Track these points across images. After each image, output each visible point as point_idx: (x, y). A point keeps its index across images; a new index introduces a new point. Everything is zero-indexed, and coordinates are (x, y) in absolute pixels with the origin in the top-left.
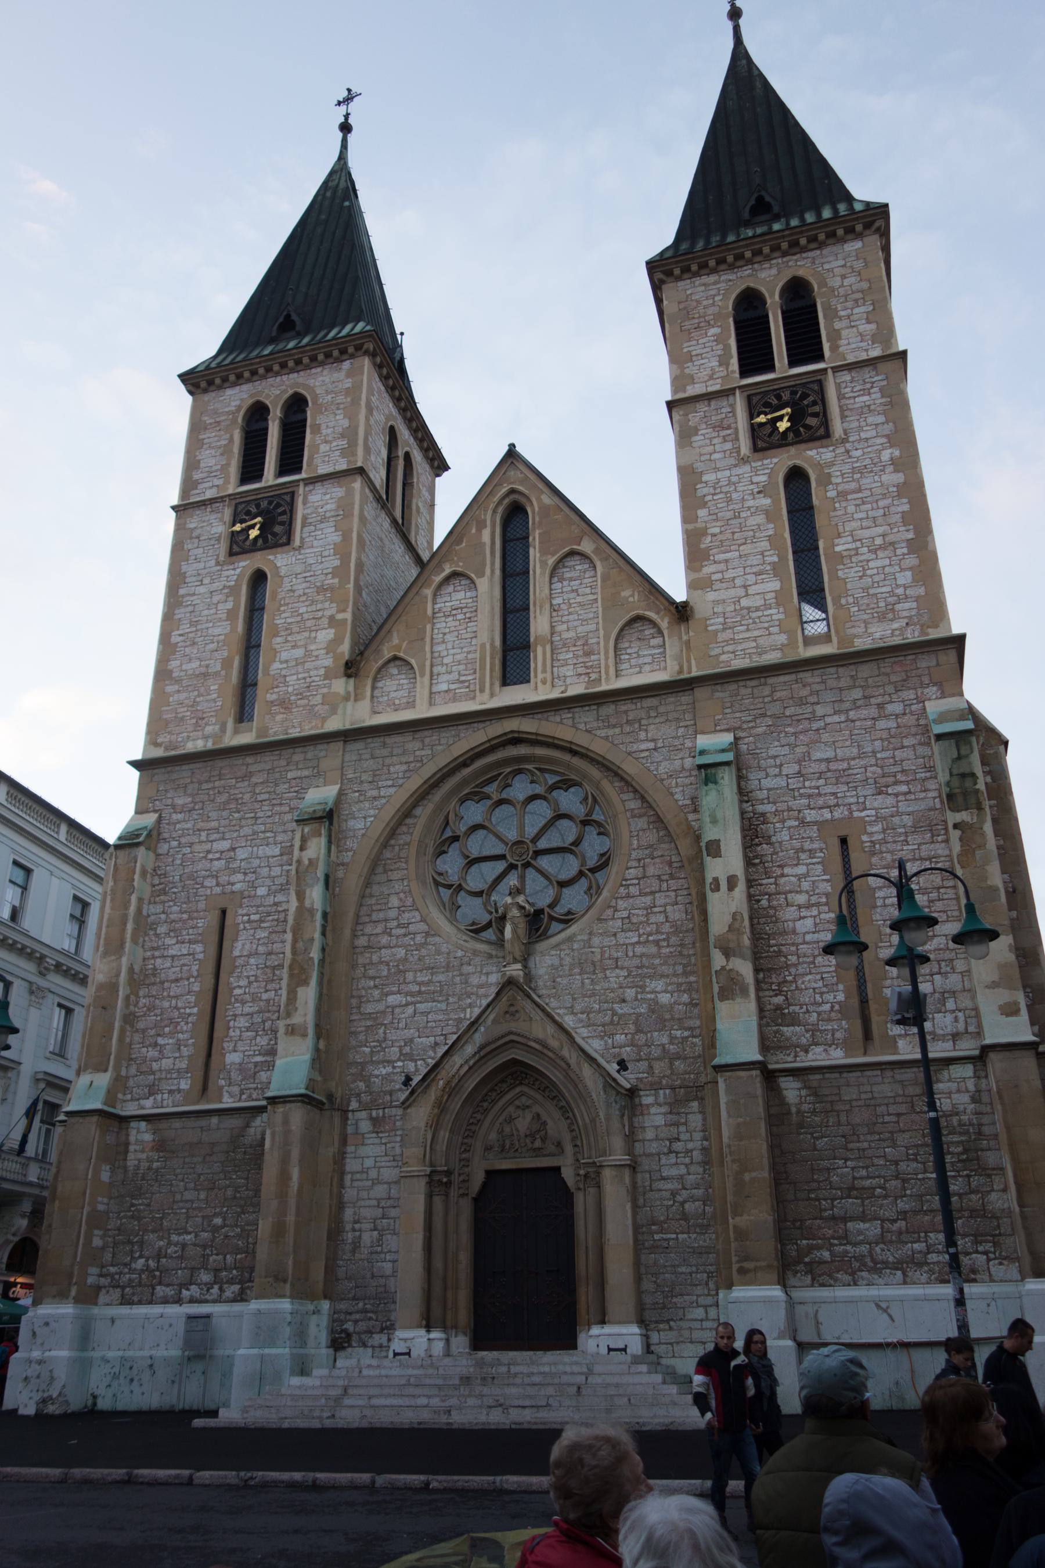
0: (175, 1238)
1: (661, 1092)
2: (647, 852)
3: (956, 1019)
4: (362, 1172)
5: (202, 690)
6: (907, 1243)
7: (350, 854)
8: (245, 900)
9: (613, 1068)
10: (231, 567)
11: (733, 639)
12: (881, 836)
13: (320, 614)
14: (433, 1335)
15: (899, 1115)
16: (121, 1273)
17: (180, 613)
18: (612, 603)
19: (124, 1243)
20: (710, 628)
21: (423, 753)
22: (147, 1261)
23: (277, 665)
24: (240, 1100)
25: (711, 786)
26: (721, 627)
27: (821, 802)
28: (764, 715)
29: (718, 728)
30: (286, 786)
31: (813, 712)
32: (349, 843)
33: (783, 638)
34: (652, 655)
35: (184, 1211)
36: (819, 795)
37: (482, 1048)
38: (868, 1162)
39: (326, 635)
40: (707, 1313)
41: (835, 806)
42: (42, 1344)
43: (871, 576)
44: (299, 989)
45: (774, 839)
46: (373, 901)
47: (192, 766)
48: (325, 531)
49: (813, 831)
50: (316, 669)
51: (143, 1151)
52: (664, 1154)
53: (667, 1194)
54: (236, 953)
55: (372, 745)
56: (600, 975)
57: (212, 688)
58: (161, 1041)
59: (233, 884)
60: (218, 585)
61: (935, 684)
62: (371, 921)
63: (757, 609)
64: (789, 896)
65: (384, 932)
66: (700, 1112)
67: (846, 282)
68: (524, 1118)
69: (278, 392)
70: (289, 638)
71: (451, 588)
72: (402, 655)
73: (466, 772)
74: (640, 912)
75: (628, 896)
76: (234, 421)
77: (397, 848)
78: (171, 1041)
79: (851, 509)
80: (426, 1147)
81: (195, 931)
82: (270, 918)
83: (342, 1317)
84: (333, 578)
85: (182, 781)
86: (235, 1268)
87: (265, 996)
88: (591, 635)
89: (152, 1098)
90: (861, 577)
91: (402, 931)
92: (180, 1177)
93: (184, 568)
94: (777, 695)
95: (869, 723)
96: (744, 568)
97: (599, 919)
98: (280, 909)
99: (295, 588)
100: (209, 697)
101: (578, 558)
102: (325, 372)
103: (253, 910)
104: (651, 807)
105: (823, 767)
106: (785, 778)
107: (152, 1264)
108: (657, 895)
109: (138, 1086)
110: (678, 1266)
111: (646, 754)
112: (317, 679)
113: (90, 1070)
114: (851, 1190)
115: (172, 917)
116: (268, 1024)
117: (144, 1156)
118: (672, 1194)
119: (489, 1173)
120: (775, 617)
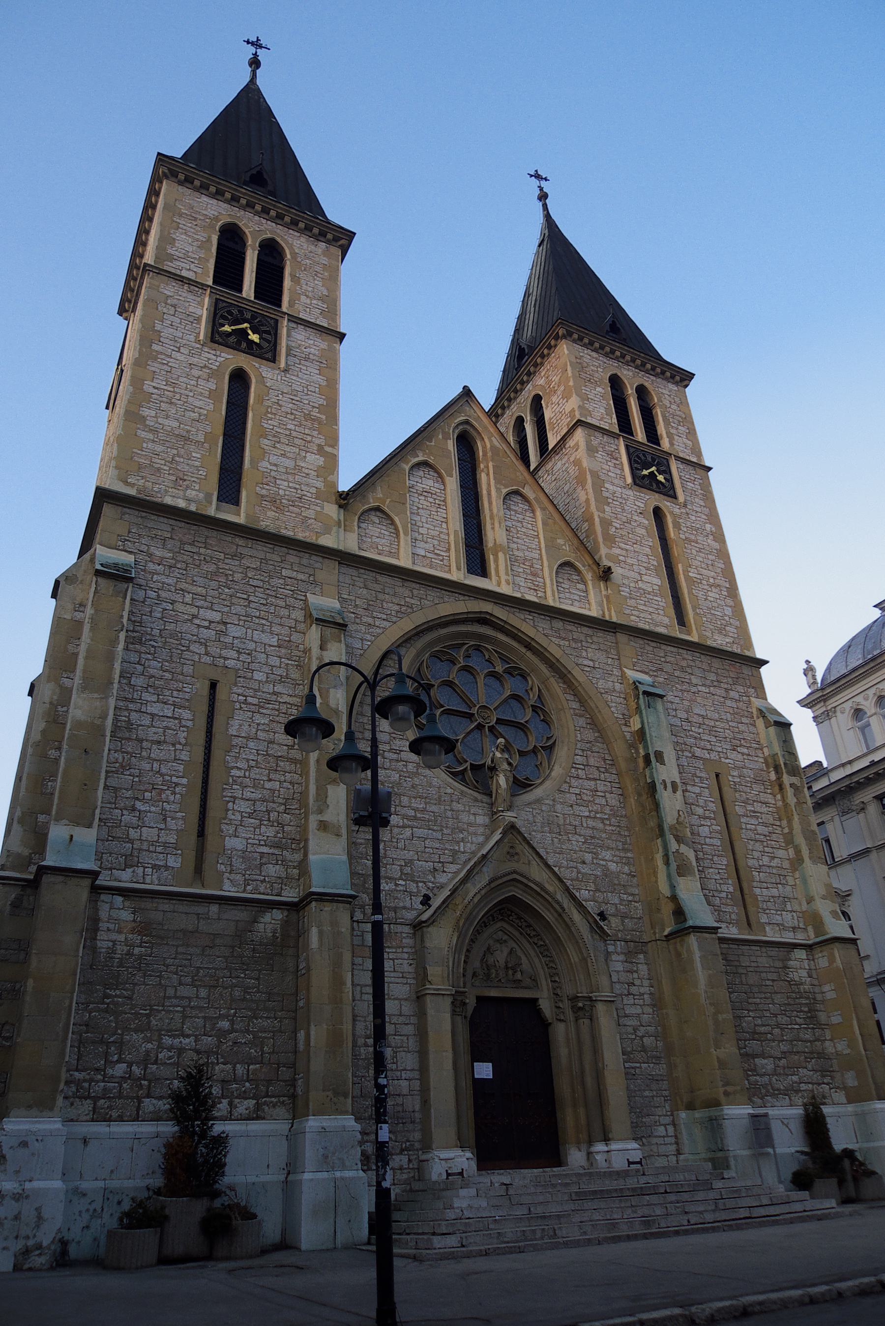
0: (167, 1041)
1: (618, 943)
2: (588, 745)
5: (182, 451)
6: (788, 1075)
8: (242, 680)
9: (598, 918)
10: (213, 352)
12: (738, 780)
13: (309, 438)
15: (773, 981)
16: (91, 1081)
17: (154, 366)
18: (551, 546)
19: (94, 1042)
20: (622, 593)
21: (413, 601)
22: (130, 1065)
23: (264, 464)
24: (244, 891)
27: (702, 743)
28: (661, 670)
30: (281, 581)
31: (690, 679)
33: (666, 620)
34: (580, 596)
35: (179, 1009)
37: (490, 882)
40: (666, 1131)
42: (17, 1172)
43: (711, 601)
47: (172, 522)
48: (310, 369)
51: (120, 932)
52: (625, 995)
53: (630, 1030)
54: (233, 731)
55: (365, 577)
56: (565, 837)
57: (194, 454)
58: (138, 805)
59: (226, 659)
60: (195, 360)
61: (753, 688)
64: (693, 807)
66: (646, 964)
67: (673, 407)
68: (502, 951)
69: (258, 229)
70: (278, 445)
71: (421, 473)
72: (386, 509)
73: (443, 631)
74: (588, 793)
75: (578, 777)
76: (212, 227)
78: (153, 809)
79: (694, 552)
80: (449, 968)
81: (181, 695)
86: (248, 1081)
87: (268, 785)
88: (534, 561)
89: (129, 871)
90: (706, 599)
91: (395, 756)
92: (172, 968)
93: (158, 327)
97: (559, 790)
99: (280, 402)
101: (520, 498)
102: (302, 239)
103: (250, 692)
107: (136, 1070)
109: (111, 853)
110: (644, 1090)
111: (588, 669)
112: (309, 494)
113: (65, 821)
115: (152, 671)
116: (273, 816)
117: (122, 938)
118: (634, 1030)
119: (480, 999)
120: (660, 603)
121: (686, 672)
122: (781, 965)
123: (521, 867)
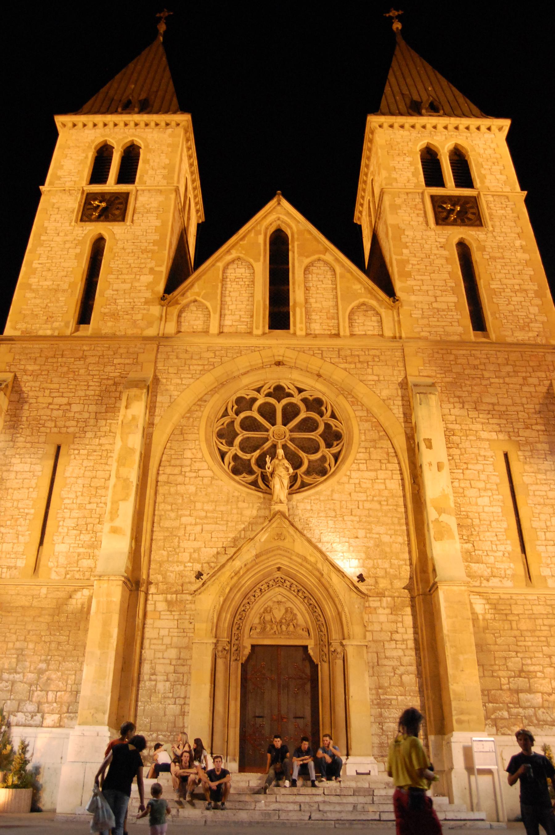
2: (372, 444)
4: (159, 638)
8: (77, 439)
25: (423, 406)
28: (451, 371)
33: (460, 329)
39: (147, 279)
44: (120, 503)
46: (173, 452)
50: (139, 298)
54: (67, 474)
59: (67, 427)
62: (170, 465)
63: (443, 310)
65: (181, 474)
68: (280, 610)
70: (120, 277)
75: (359, 470)
77: (191, 420)
82: (95, 453)
84: (154, 245)
85: (33, 355)
87: (88, 506)
94: (459, 361)
97: (338, 482)
98: (104, 448)
100: (58, 305)
104: (373, 416)
108: (379, 472)
116: (90, 527)
119: (253, 646)
121: (478, 369)
123: (286, 544)
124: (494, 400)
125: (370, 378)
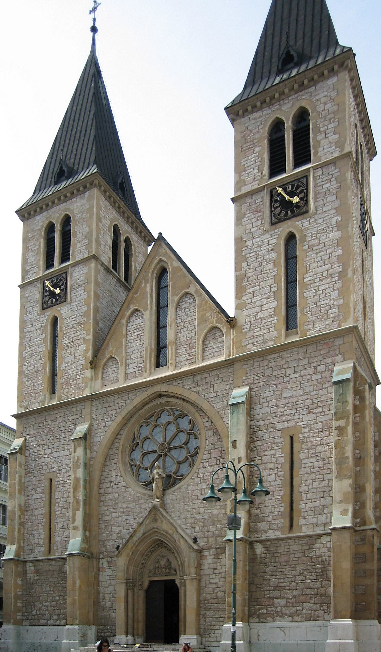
0: (44, 604)
3: (327, 517)
7: (95, 453)
11: (253, 336)
12: (306, 434)
14: (128, 638)
15: (299, 558)
26: (248, 329)
27: (284, 418)
28: (264, 376)
29: (243, 384)
31: (285, 373)
32: (95, 448)
33: (275, 334)
36: (284, 415)
38: (285, 576)
41: (290, 420)
45: (262, 438)
46: (105, 473)
49: (279, 434)
77: (114, 449)
83: (100, 631)
94: (270, 365)
95: (309, 377)
96: (261, 295)
105: (286, 401)
106: (270, 407)
114: (277, 587)
120: (273, 322)
121: (283, 368)
122: (307, 547)
124: (290, 394)
125: (212, 395)
